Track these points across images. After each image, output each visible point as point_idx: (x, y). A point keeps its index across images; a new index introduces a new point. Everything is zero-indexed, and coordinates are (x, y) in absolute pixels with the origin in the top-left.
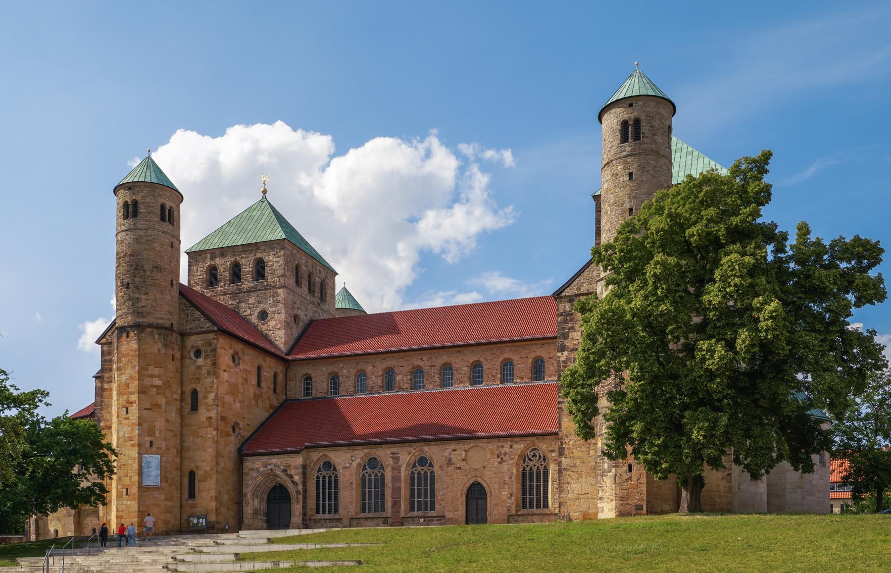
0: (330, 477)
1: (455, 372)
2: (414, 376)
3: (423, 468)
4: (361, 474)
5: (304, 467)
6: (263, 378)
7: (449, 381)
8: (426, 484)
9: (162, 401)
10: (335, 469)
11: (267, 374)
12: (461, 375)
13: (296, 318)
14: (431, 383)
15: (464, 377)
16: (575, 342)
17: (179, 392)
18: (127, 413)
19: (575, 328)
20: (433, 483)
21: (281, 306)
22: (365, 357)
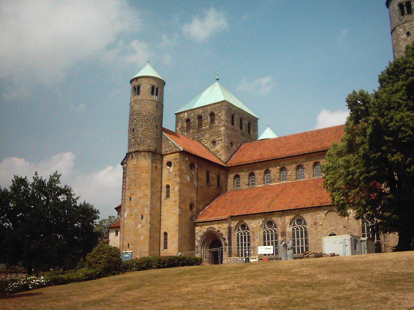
0: (245, 234)
3: (300, 226)
4: (263, 231)
5: (230, 229)
6: (210, 178)
8: (298, 237)
9: (148, 192)
10: (248, 229)
11: (213, 175)
13: (232, 144)
17: (160, 187)
18: (130, 200)
20: (306, 236)
21: (222, 138)
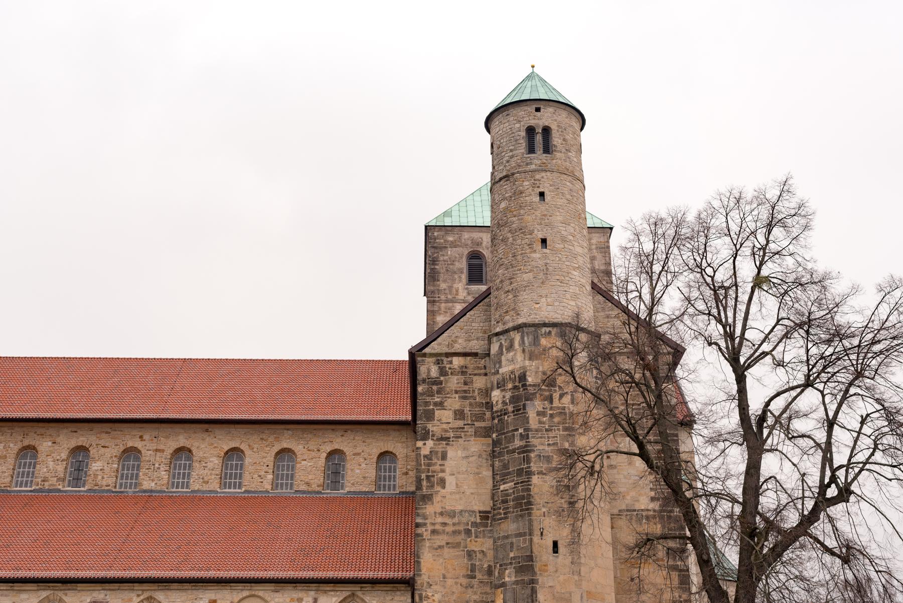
1: (196, 465)
2: (123, 465)
7: (184, 478)
12: (206, 471)
14: (153, 480)
15: (211, 474)
16: (444, 426)
19: (446, 404)
22: (41, 424)
